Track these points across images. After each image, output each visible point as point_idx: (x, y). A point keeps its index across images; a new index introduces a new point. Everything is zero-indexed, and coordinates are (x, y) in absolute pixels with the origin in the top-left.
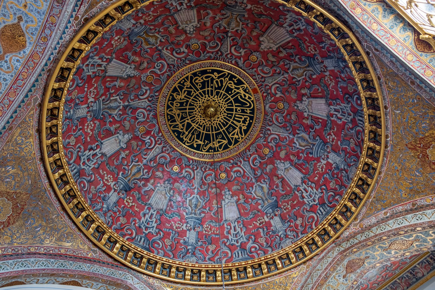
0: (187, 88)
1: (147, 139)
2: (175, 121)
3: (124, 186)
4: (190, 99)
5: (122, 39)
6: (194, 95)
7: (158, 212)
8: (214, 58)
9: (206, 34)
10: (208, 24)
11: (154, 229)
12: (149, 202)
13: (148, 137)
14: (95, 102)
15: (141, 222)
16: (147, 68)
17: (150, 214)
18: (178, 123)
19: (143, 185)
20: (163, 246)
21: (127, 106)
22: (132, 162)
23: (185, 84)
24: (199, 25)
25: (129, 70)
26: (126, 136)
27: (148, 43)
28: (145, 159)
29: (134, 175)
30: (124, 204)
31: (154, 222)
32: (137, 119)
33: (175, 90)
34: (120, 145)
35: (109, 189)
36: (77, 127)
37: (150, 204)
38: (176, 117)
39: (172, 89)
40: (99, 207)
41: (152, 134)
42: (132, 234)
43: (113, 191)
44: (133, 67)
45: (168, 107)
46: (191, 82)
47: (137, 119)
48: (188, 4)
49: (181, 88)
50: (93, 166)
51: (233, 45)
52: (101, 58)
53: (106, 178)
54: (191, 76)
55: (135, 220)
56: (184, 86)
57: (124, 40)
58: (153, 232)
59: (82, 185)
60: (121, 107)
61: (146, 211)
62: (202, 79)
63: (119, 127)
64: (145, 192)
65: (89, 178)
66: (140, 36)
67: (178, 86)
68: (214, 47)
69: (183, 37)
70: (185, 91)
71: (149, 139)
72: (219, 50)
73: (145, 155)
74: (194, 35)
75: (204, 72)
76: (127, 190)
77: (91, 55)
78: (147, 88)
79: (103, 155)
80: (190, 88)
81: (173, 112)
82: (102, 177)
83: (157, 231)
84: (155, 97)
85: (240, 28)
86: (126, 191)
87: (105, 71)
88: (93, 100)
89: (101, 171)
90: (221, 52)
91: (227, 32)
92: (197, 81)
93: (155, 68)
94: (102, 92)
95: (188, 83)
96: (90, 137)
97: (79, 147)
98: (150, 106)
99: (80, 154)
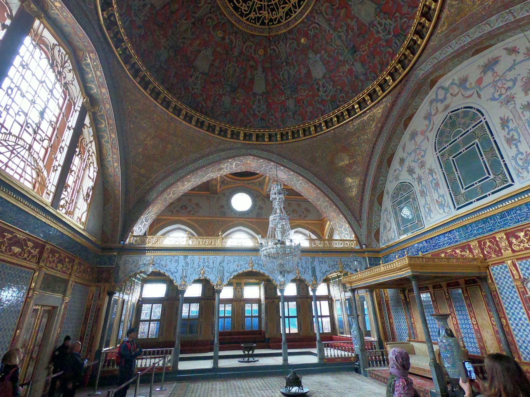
0: (256, 14)
1: (311, 33)
2: (290, 10)
3: (352, 54)
4: (265, 5)
5: (238, 95)
6: (259, 3)
7: (377, 15)
8: (219, 10)
9: (205, 35)
10: (198, 42)
11: (391, 23)
12: (368, 25)
13: (310, 32)
14: (285, 93)
15: (383, 38)
16: (253, 58)
17: (378, 26)
18: (291, 6)
19: (352, 32)
20: (406, 17)
21: (286, 62)
22: (331, 45)
23: (254, 18)
24: (203, 48)
25: (259, 73)
26: (310, 56)
27: (235, 71)
28: (329, 31)
29: (342, 41)
30: (364, 56)
31: (386, 22)
32: (295, 49)
33: (263, 23)
34: (318, 61)
35: (350, 71)
36: (300, 106)
37: (370, 24)
38: (286, 9)
39: (263, 27)
40: (360, 84)
41: (306, 29)
42: (389, 52)
43: (353, 67)
44: (255, 72)
45: (279, 22)
46: (250, 13)
47: (295, 49)
48: (194, 73)
49: (259, 18)
50: (331, 87)
51: (198, 7)
52: (254, 102)
53: (342, 74)
54: (245, 17)
55: (381, 45)
56: (255, 17)
57: (238, 93)
58: (394, 25)
59: (341, 99)
60: (288, 68)
61: (373, 30)
62: (242, 6)
63: (303, 65)
64: (358, 30)
65: (339, 91)
66: (232, 82)
67: (258, 22)
68: (210, 18)
69: (219, 49)
70: (260, 14)
71: (311, 30)
72: (211, 13)
73: (326, 32)
74: (213, 43)
75: (236, 8)
76: (354, 50)
77: (252, 113)
78: (269, 50)
79: (324, 77)
80: (255, 11)
81: (282, 15)
82: (340, 76)
83: (394, 20)
84: (274, 38)
85: (182, 20)
86: (355, 52)
87: (262, 94)
88: (283, 96)
89: (336, 79)
90: (211, 10)
91: (193, 23)
92: (247, 9)
93: (251, 53)
94: (277, 90)
95: (252, 15)
96: (310, 91)
97: (315, 102)
98: (283, 40)
99: (320, 101)
